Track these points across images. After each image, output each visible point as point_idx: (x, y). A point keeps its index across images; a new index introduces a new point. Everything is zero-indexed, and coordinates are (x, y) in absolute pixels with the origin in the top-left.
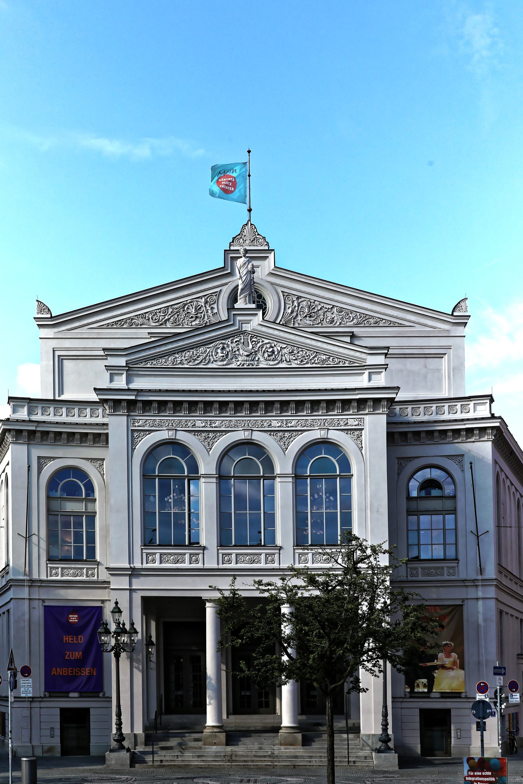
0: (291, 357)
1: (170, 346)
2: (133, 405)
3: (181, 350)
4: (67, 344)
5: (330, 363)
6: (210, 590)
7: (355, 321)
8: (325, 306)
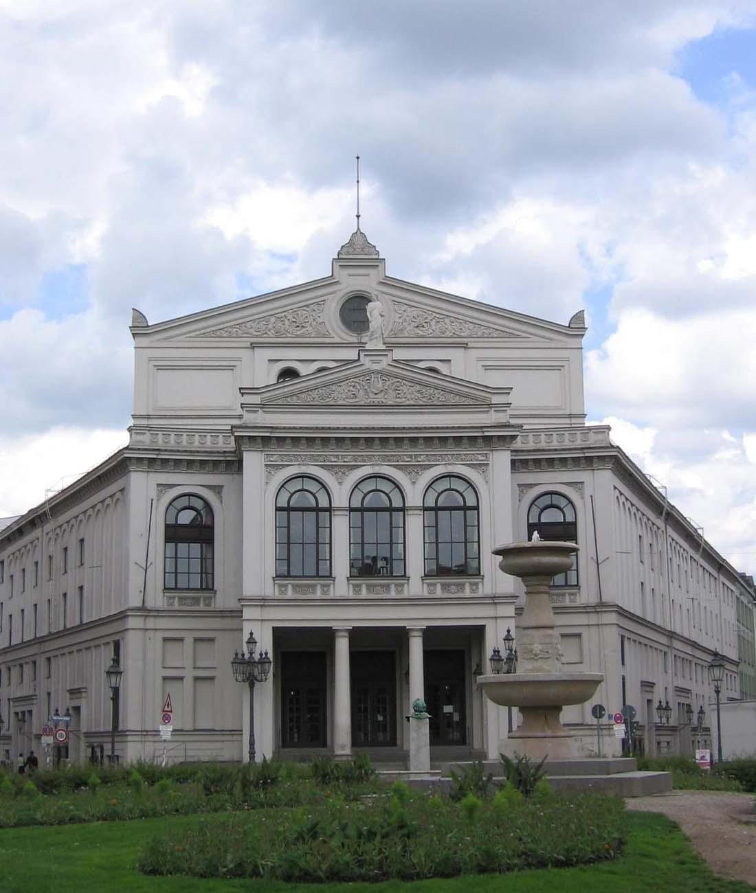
0: (420, 395)
2: (267, 441)
8: (438, 316)
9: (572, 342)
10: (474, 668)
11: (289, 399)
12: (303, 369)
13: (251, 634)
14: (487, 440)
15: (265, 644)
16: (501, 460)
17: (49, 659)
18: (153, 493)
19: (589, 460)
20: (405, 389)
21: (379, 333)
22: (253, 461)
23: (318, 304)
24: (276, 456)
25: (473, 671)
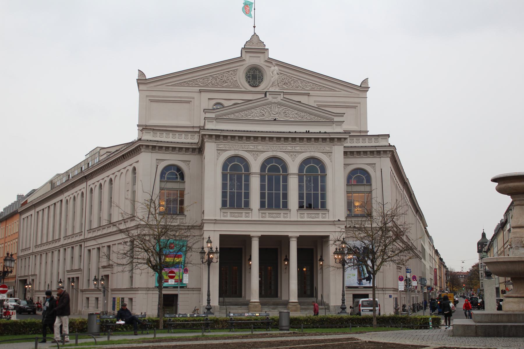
1: (237, 108)
2: (218, 137)
3: (242, 111)
4: (154, 93)
5: (316, 119)
6: (256, 231)
7: (310, 87)
9: (361, 94)
10: (319, 258)
11: (229, 116)
12: (226, 103)
13: (209, 238)
14: (332, 140)
15: (216, 244)
16: (338, 150)
17: (89, 251)
18: (154, 162)
19: (379, 152)
20: (290, 112)
21: (277, 83)
22: (210, 147)
23: (234, 71)
24: (223, 145)
25: (319, 259)
